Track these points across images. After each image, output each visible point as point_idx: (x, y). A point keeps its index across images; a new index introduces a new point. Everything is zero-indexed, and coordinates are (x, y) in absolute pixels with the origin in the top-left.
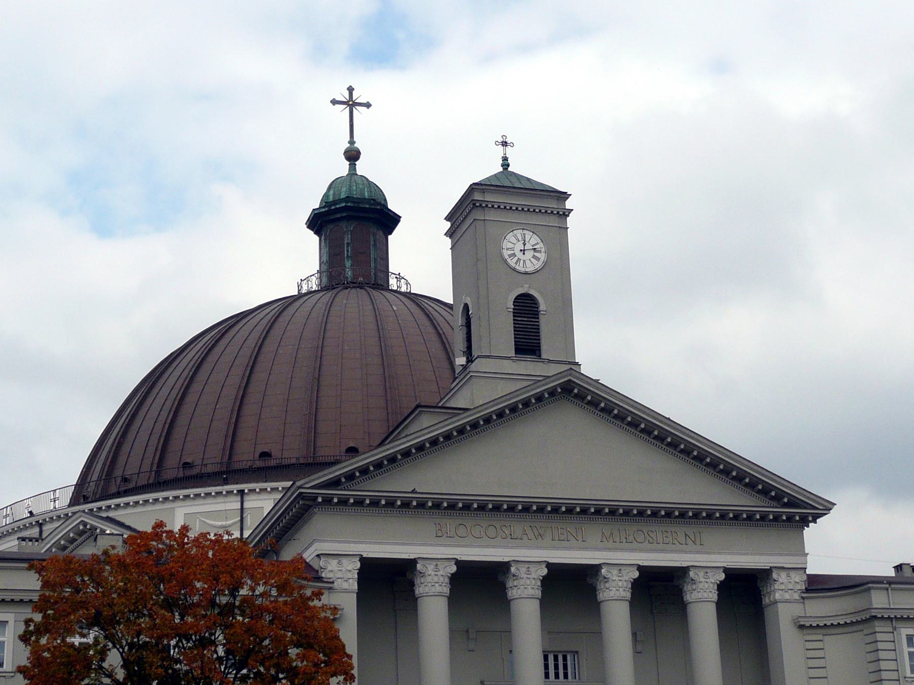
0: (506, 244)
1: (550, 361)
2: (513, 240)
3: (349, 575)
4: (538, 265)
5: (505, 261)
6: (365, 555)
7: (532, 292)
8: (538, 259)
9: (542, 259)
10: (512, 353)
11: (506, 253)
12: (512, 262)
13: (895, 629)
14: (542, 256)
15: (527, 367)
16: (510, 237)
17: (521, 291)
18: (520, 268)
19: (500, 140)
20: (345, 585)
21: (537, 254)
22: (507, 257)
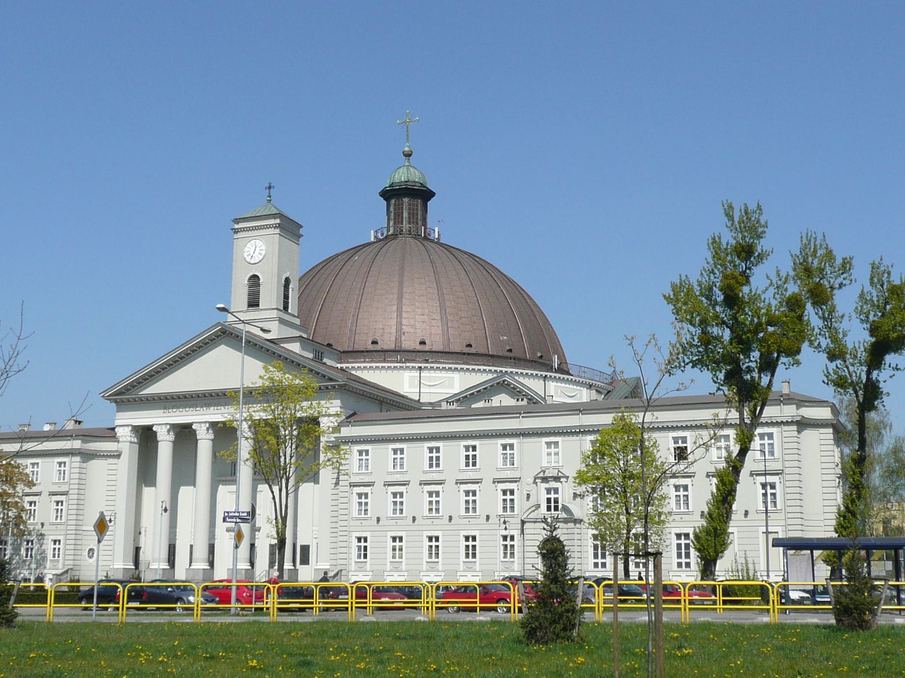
0: (246, 249)
1: (262, 310)
2: (250, 246)
3: (127, 434)
4: (261, 257)
5: (245, 259)
6: (134, 424)
7: (256, 274)
8: (260, 254)
9: (263, 254)
10: (245, 307)
11: (245, 255)
12: (248, 259)
13: (350, 447)
14: (263, 253)
15: (252, 315)
16: (249, 245)
17: (252, 274)
18: (252, 262)
19: (268, 186)
20: (125, 439)
21: (261, 252)
22: (246, 256)
